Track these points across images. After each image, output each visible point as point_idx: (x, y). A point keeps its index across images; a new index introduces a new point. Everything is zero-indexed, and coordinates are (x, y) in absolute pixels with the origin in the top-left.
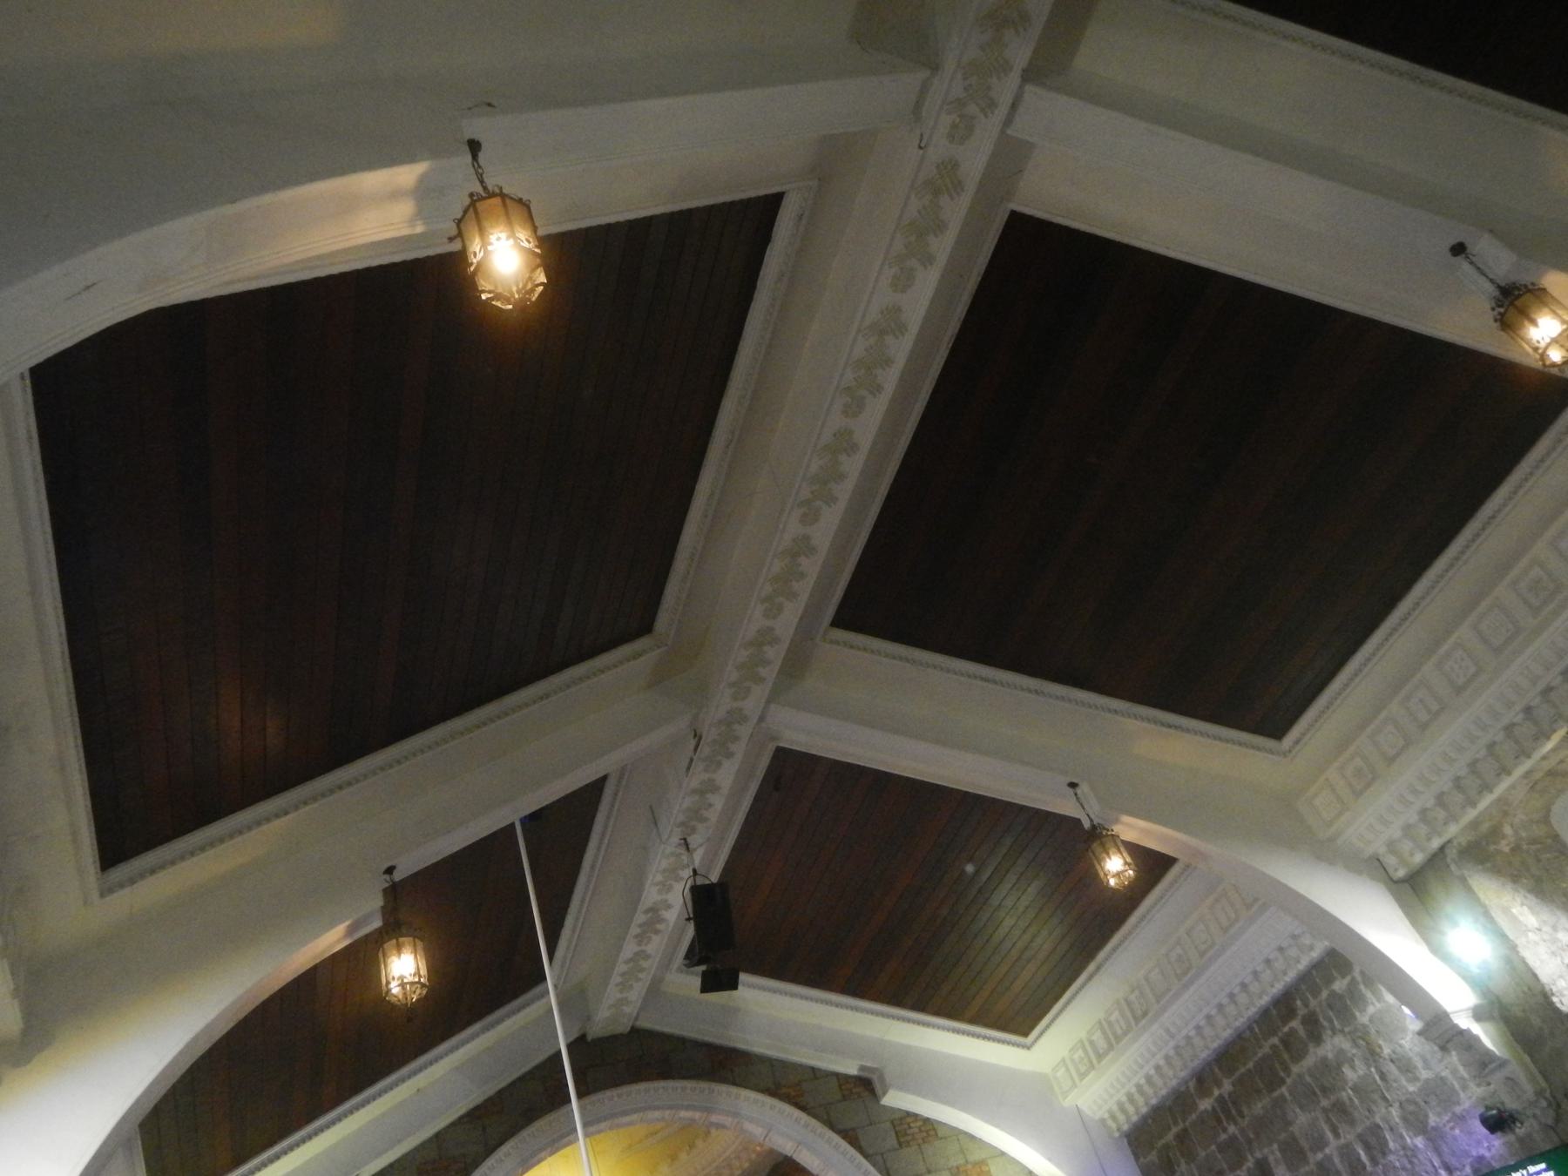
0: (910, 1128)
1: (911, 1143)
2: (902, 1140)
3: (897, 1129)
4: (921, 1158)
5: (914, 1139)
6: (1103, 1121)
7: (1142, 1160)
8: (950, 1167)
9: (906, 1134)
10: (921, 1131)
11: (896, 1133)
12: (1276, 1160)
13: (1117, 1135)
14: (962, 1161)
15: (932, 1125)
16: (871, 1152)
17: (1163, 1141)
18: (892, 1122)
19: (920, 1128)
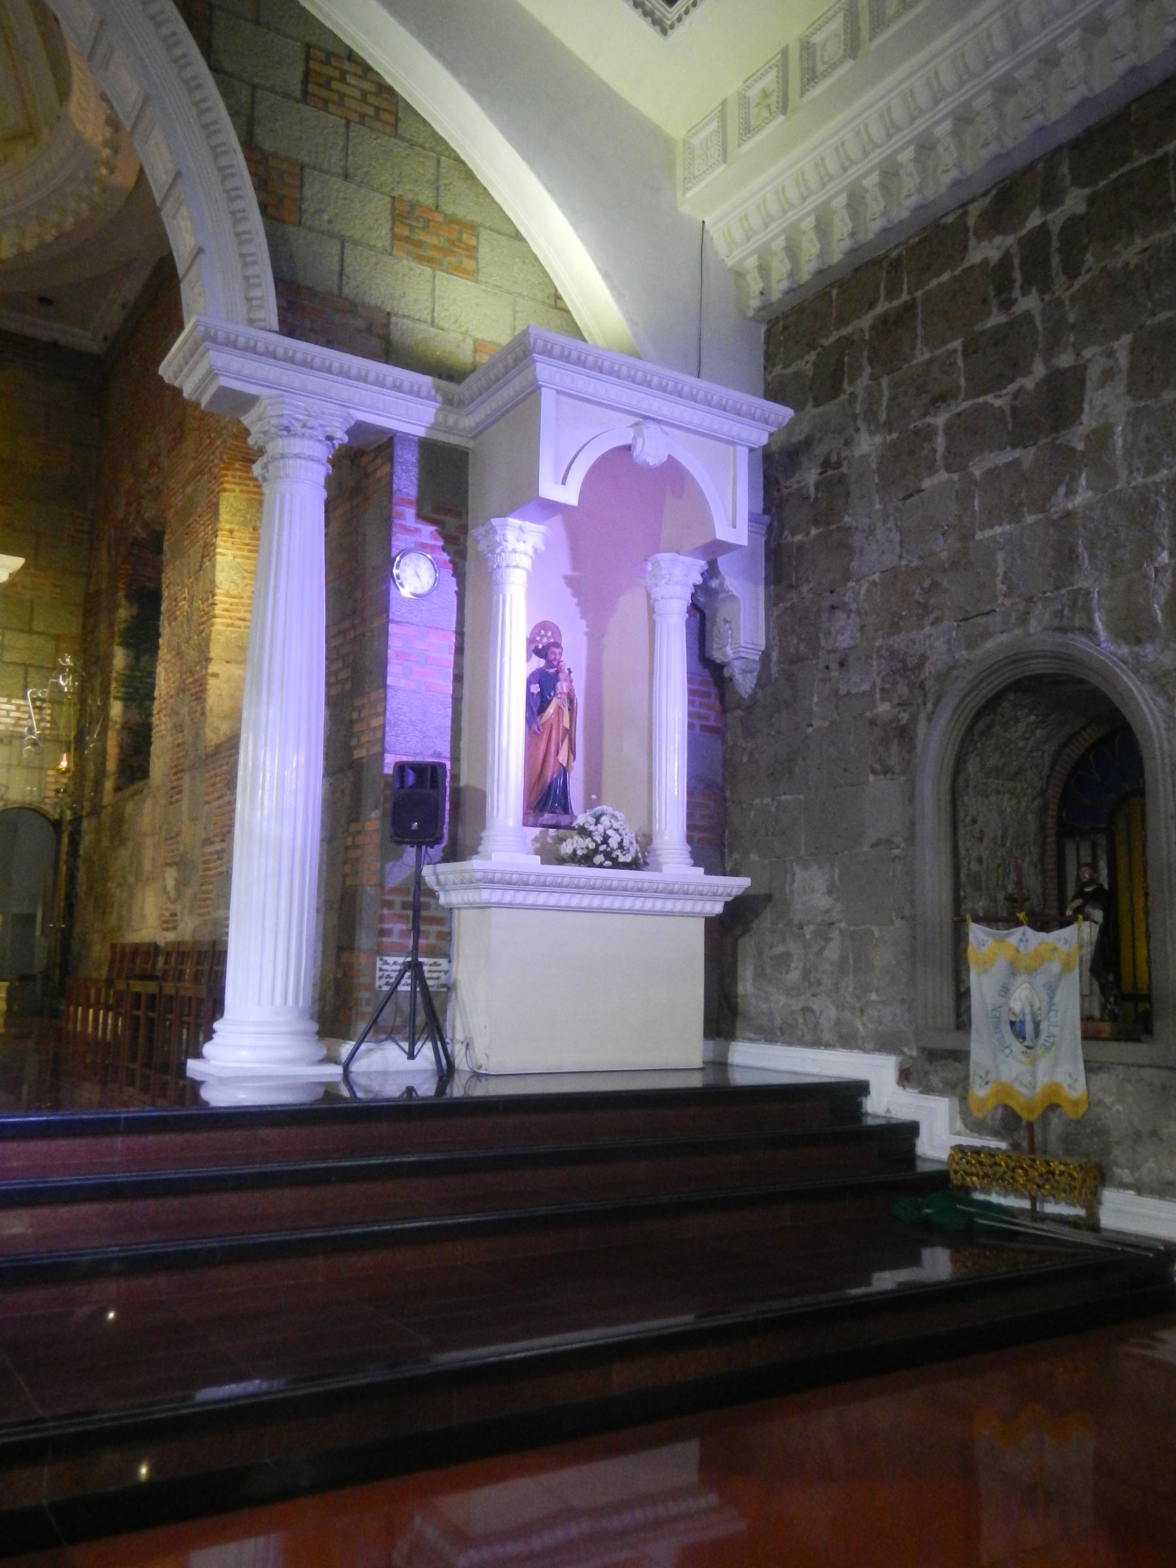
0: (342, 80)
1: (332, 107)
2: (312, 88)
3: (313, 66)
4: (341, 143)
5: (341, 104)
6: (739, 275)
7: (778, 370)
8: (394, 194)
9: (328, 87)
10: (364, 99)
11: (307, 72)
12: (1108, 375)
13: (755, 303)
14: (426, 198)
15: (396, 104)
16: (228, 67)
17: (844, 332)
18: (308, 47)
19: (365, 93)
